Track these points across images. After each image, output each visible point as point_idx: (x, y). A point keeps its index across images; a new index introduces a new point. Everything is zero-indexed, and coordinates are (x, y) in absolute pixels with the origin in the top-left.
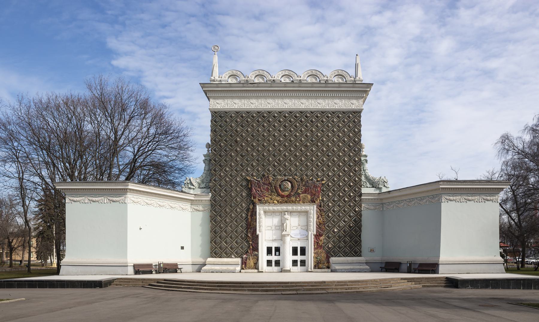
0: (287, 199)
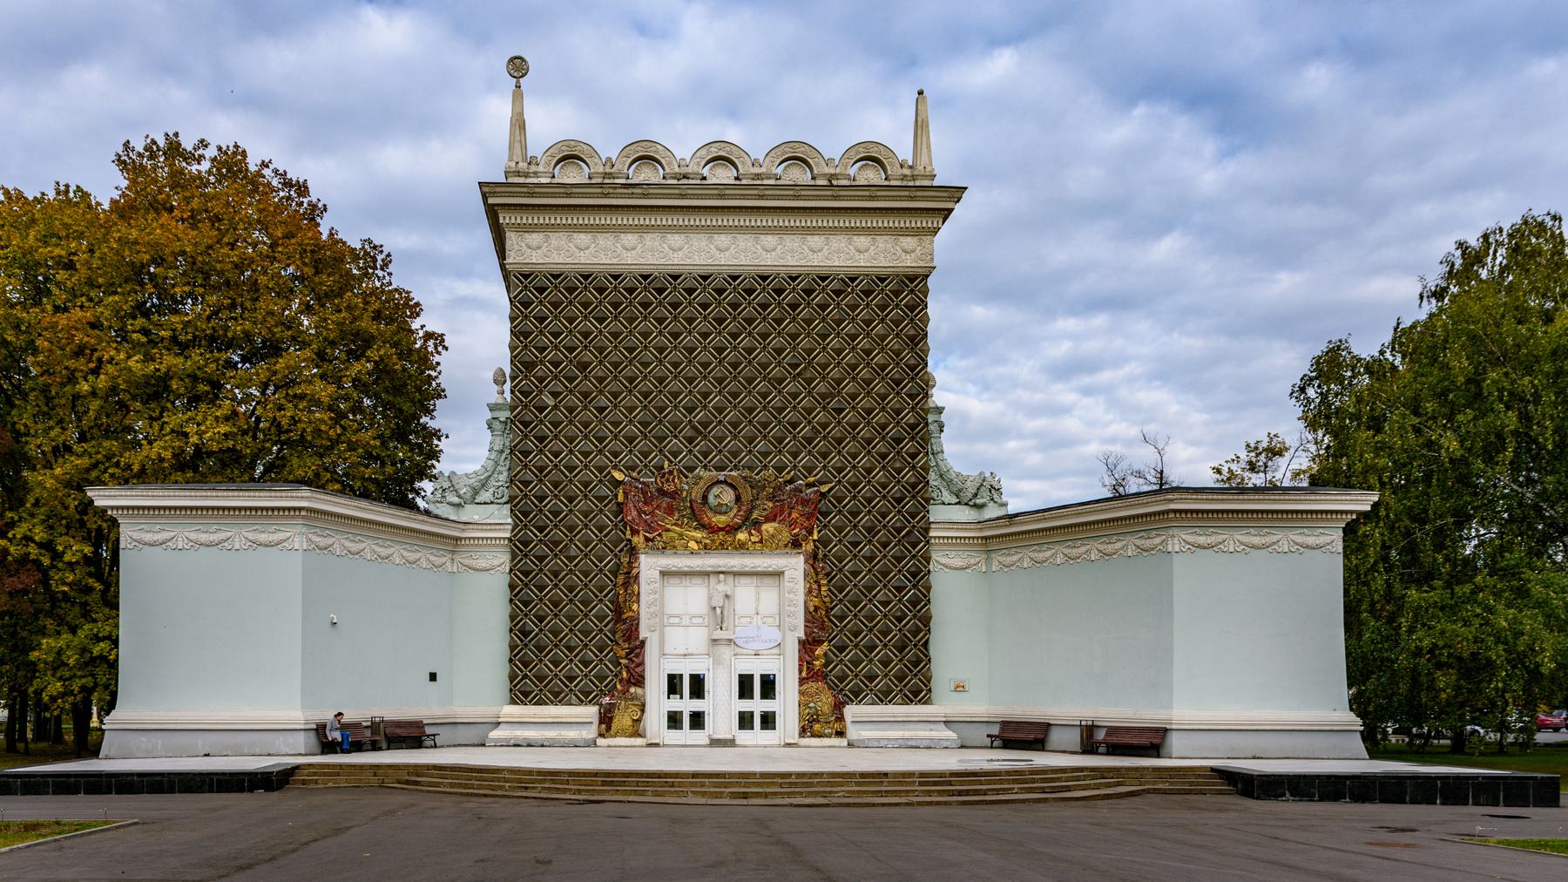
0: (722, 538)
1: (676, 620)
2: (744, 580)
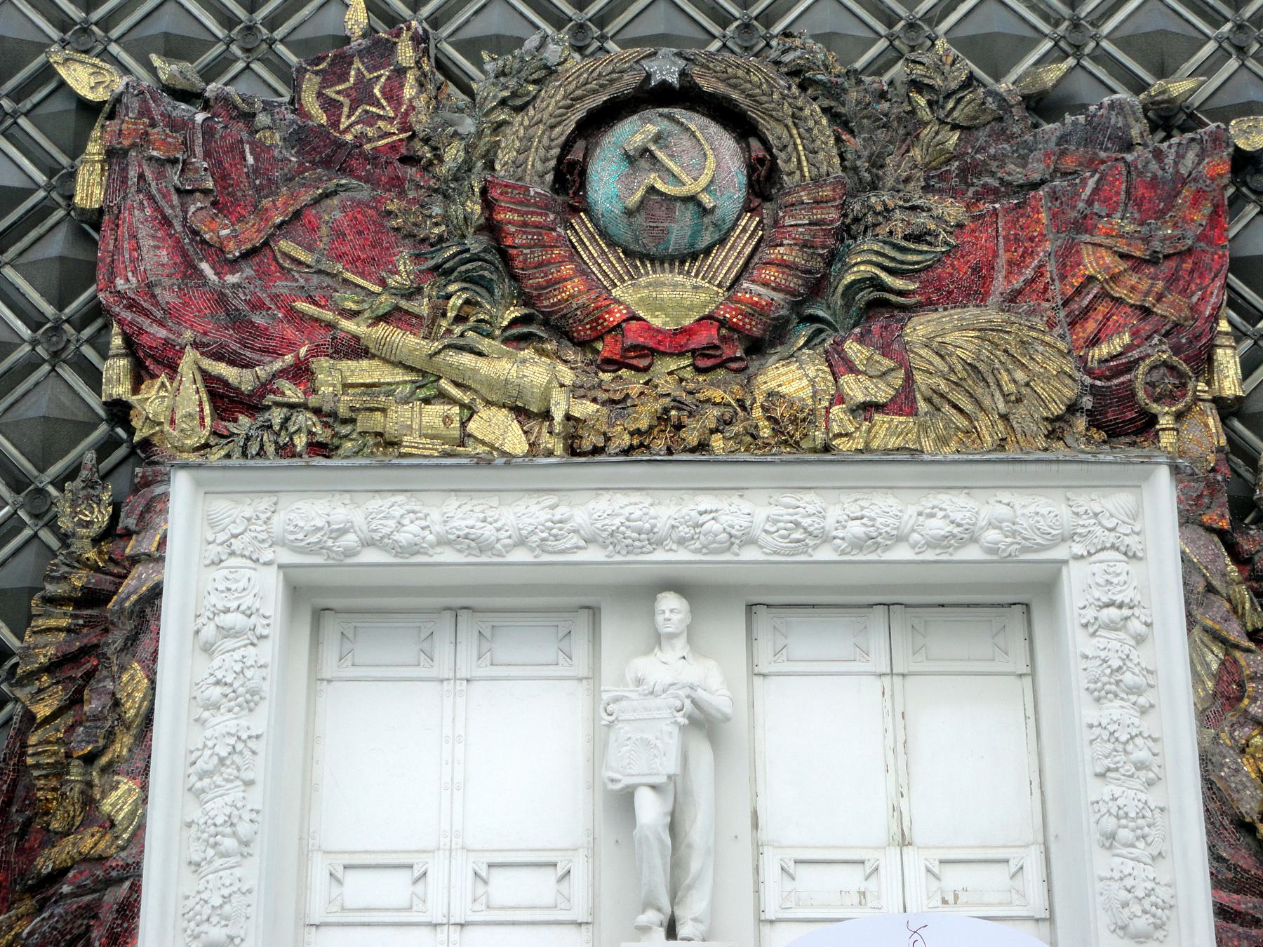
1: (389, 890)
2: (814, 642)
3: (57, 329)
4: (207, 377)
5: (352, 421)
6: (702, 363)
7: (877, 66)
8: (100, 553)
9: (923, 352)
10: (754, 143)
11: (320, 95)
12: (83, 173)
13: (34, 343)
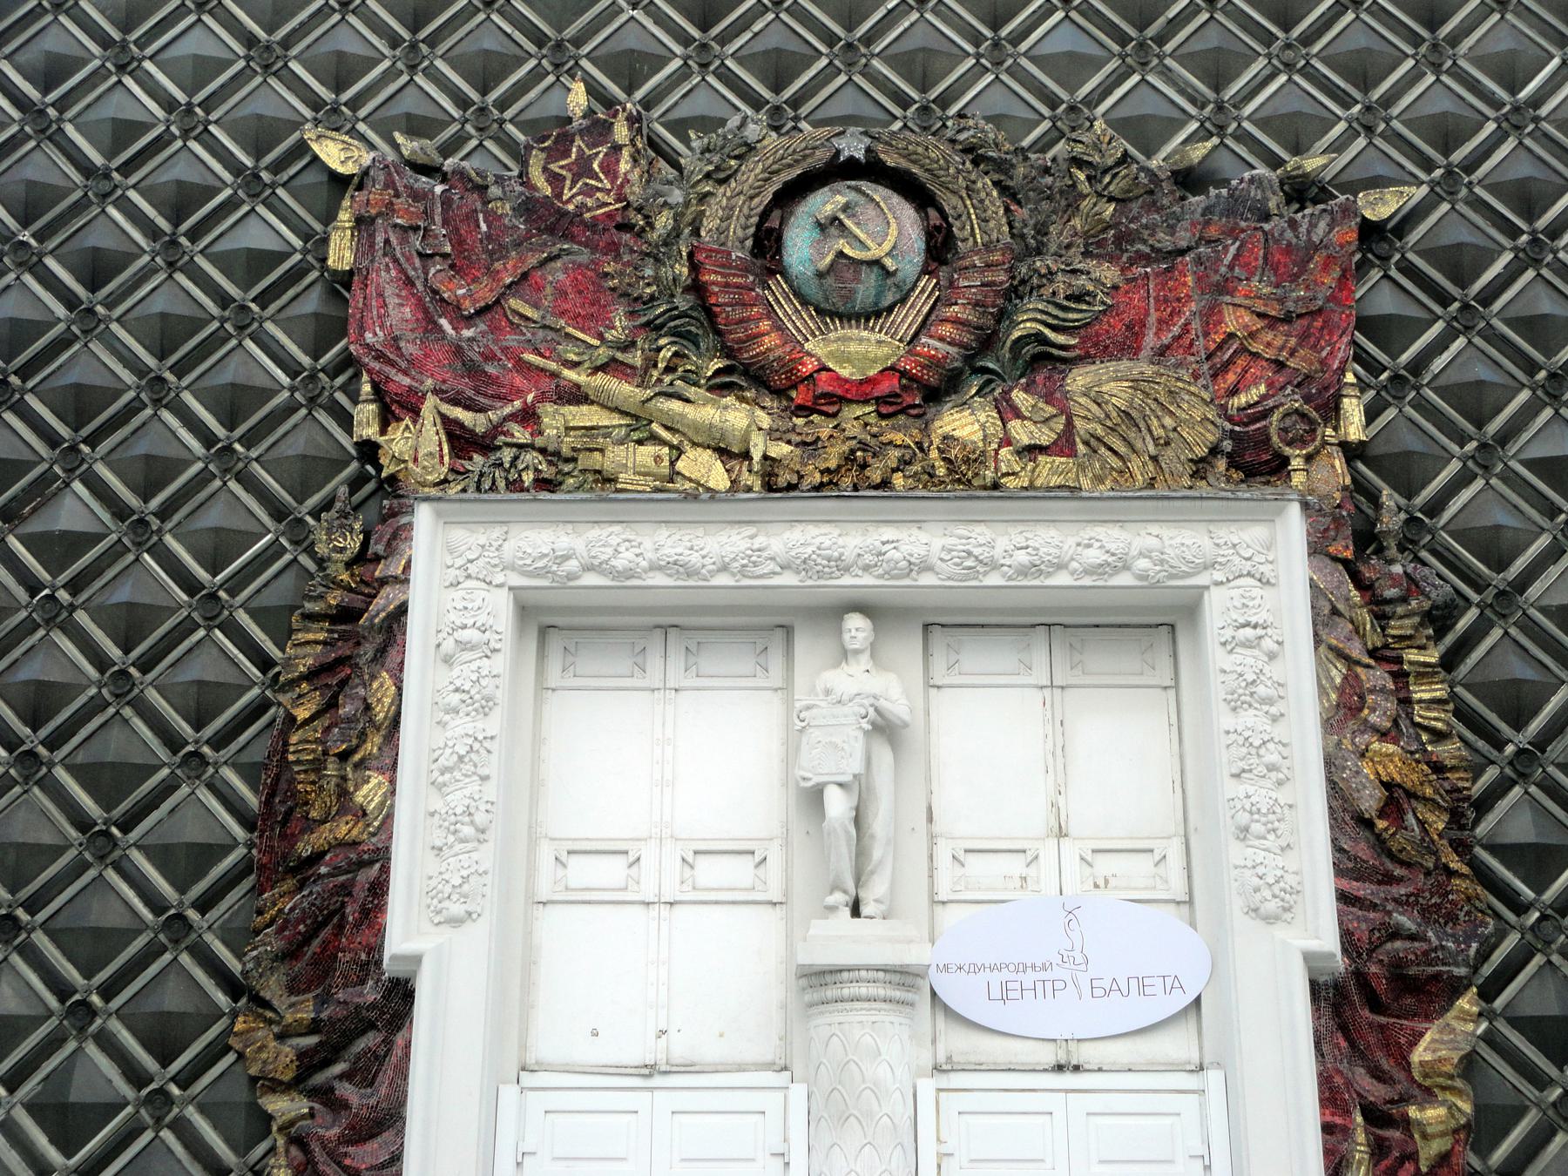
0: (863, 441)
1: (609, 872)
3: (313, 377)
4: (446, 420)
5: (574, 460)
6: (884, 410)
7: (1043, 145)
8: (352, 575)
9: (1082, 400)
10: (932, 213)
11: (545, 169)
12: (335, 238)
13: (293, 389)
